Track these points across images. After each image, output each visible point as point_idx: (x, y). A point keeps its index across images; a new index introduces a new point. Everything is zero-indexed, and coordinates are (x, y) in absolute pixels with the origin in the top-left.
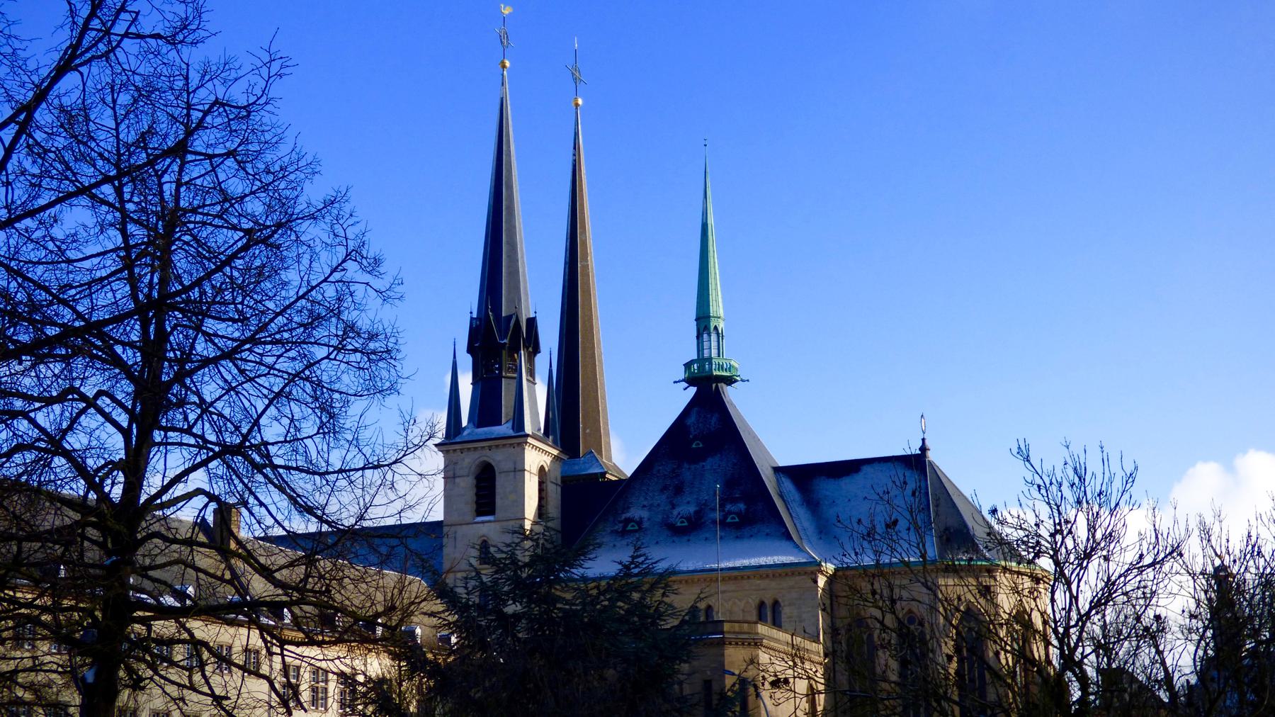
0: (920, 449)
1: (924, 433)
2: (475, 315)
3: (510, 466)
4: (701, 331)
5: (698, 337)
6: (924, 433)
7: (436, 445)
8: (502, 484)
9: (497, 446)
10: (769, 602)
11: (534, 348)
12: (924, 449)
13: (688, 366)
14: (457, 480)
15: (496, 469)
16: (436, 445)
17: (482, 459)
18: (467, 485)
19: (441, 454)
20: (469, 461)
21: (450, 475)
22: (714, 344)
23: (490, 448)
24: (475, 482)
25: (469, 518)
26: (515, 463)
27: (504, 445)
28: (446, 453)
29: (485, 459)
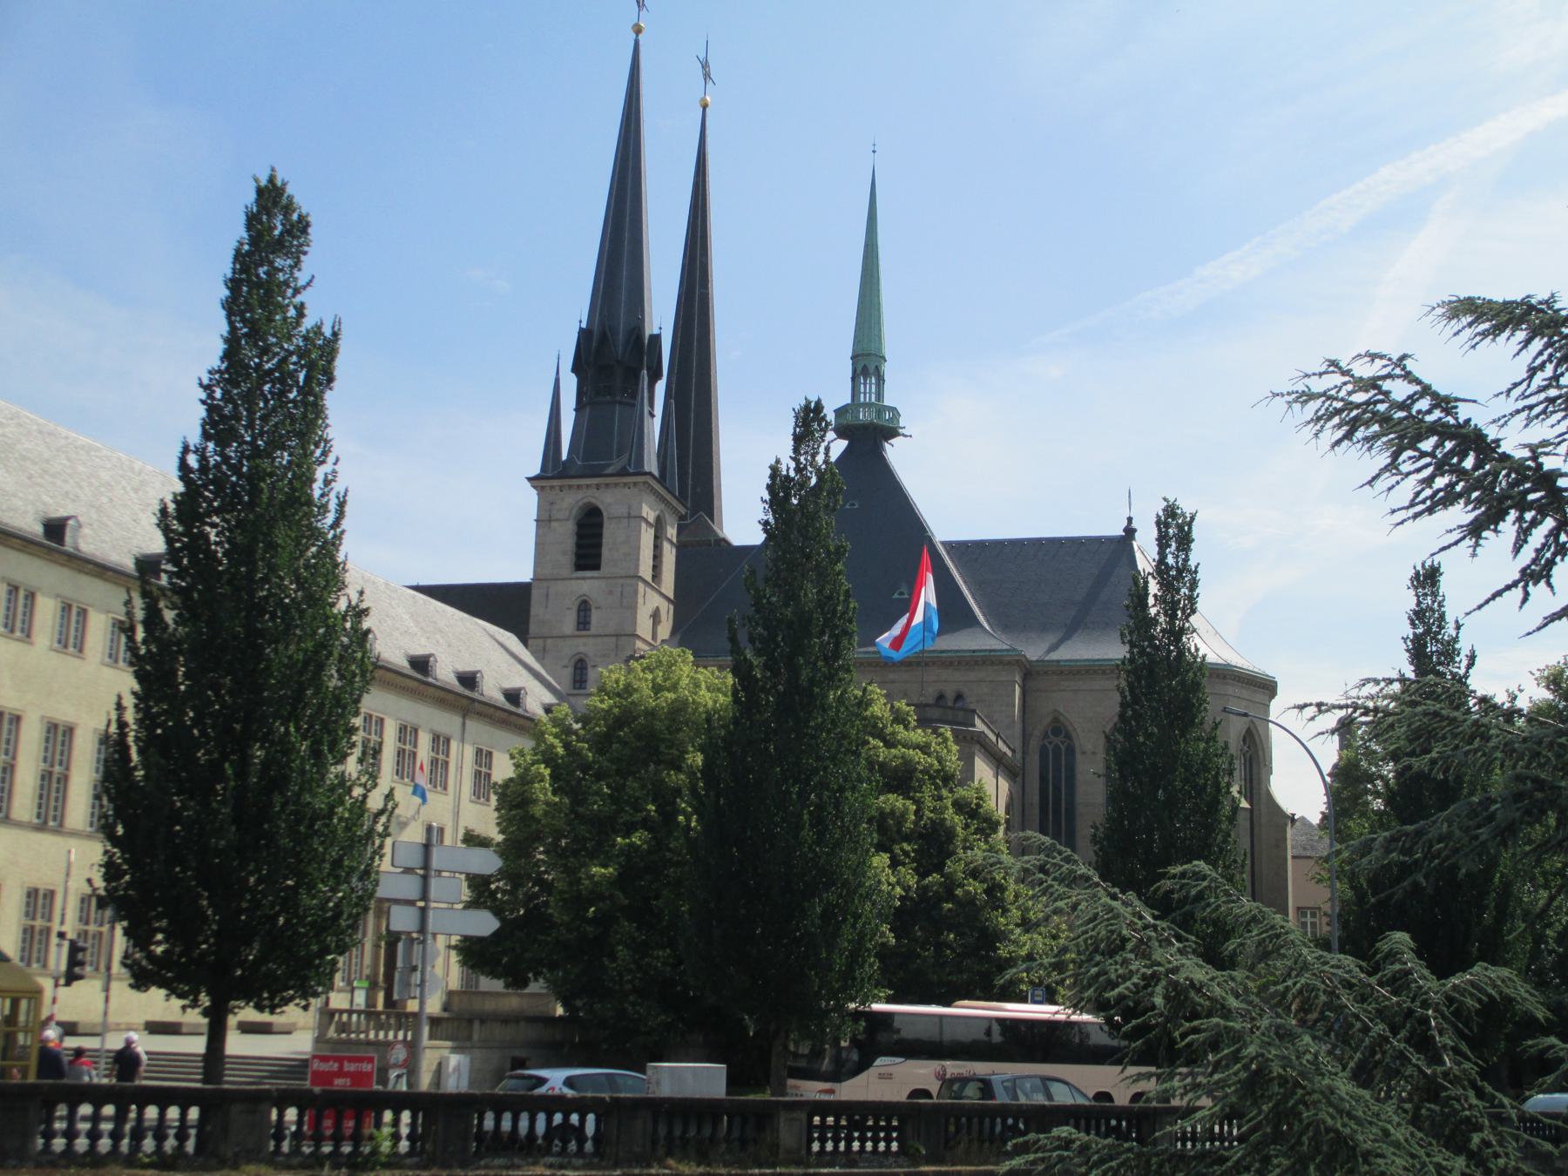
0: (1125, 530)
2: (584, 325)
3: (623, 511)
5: (853, 379)
7: (529, 479)
8: (611, 534)
9: (607, 485)
14: (554, 524)
15: (605, 514)
16: (529, 479)
17: (586, 500)
18: (566, 533)
19: (534, 492)
20: (571, 501)
21: (543, 521)
23: (598, 487)
24: (575, 528)
26: (630, 507)
28: (541, 490)
29: (594, 501)
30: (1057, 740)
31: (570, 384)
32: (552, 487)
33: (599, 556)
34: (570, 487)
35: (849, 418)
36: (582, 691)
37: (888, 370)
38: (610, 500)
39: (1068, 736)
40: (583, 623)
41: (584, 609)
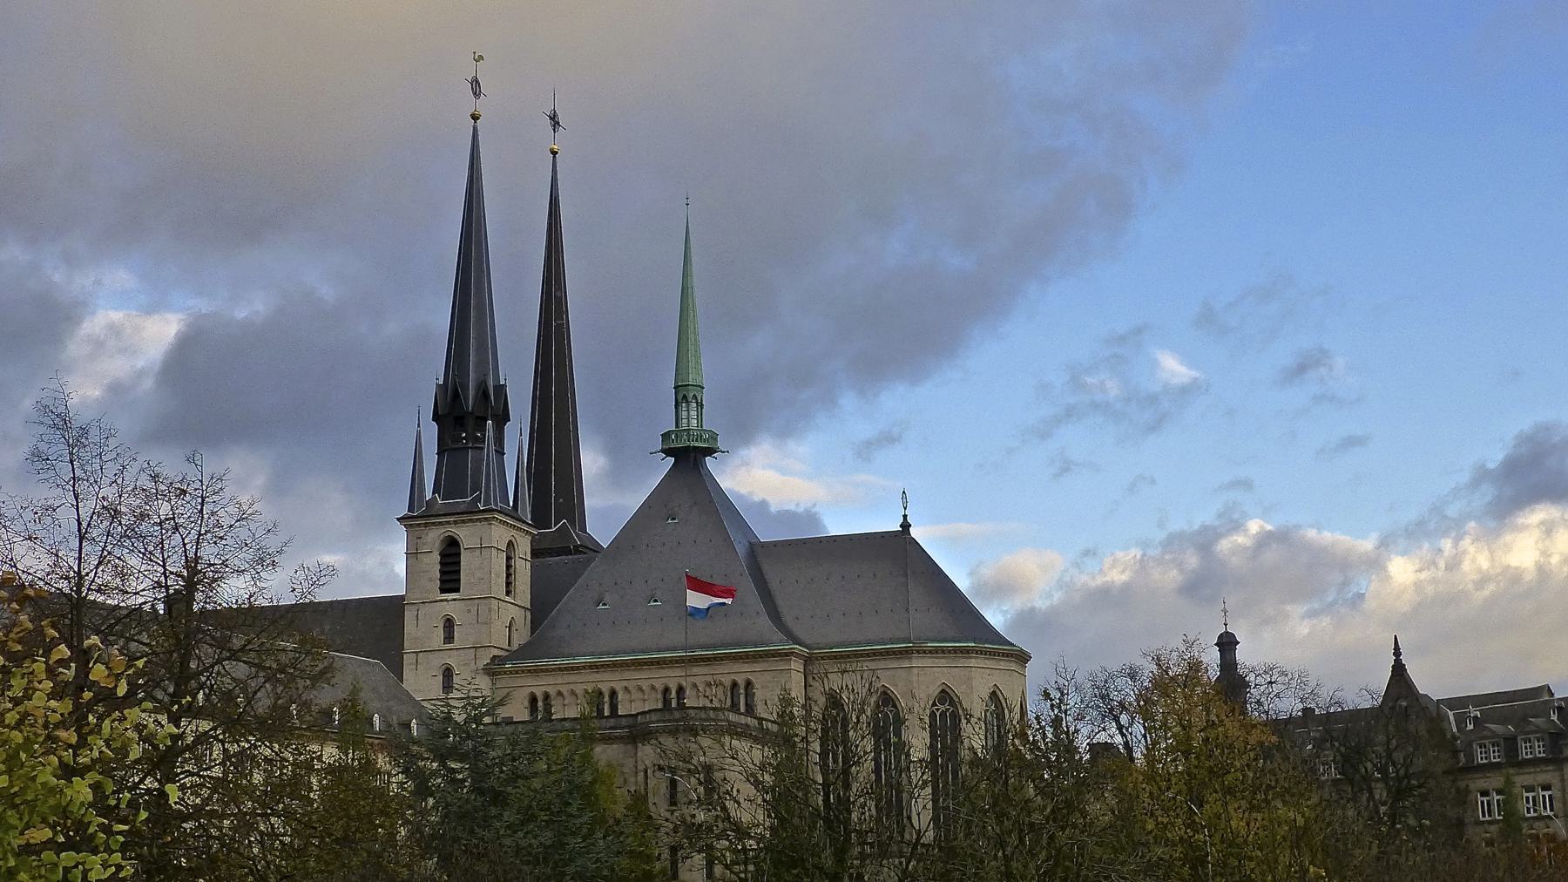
0: (901, 526)
1: (905, 508)
6: (905, 508)
7: (398, 519)
9: (463, 521)
10: (741, 683)
11: (502, 418)
12: (906, 526)
13: (666, 436)
16: (398, 519)
18: (433, 563)
20: (434, 538)
22: (693, 413)
23: (456, 522)
29: (450, 534)
31: (431, 432)
33: (459, 580)
40: (449, 638)
41: (449, 624)
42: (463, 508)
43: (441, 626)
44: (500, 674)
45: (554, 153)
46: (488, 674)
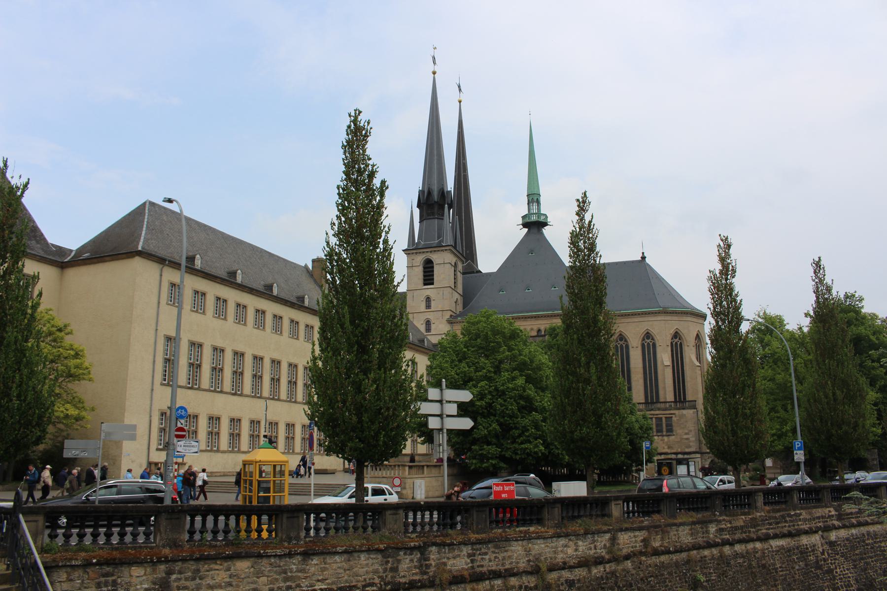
2: (421, 189)
4: (530, 201)
5: (528, 204)
7: (403, 250)
8: (437, 270)
9: (435, 251)
12: (643, 258)
13: (523, 217)
14: (414, 268)
16: (403, 250)
18: (419, 271)
20: (420, 259)
23: (431, 252)
25: (421, 286)
27: (438, 251)
28: (408, 254)
29: (429, 257)
30: (621, 343)
32: (413, 253)
34: (420, 253)
35: (527, 220)
36: (430, 333)
37: (542, 200)
38: (436, 258)
39: (626, 341)
40: (428, 306)
41: (428, 300)
42: (435, 245)
43: (425, 301)
44: (454, 323)
45: (460, 102)
46: (449, 323)
